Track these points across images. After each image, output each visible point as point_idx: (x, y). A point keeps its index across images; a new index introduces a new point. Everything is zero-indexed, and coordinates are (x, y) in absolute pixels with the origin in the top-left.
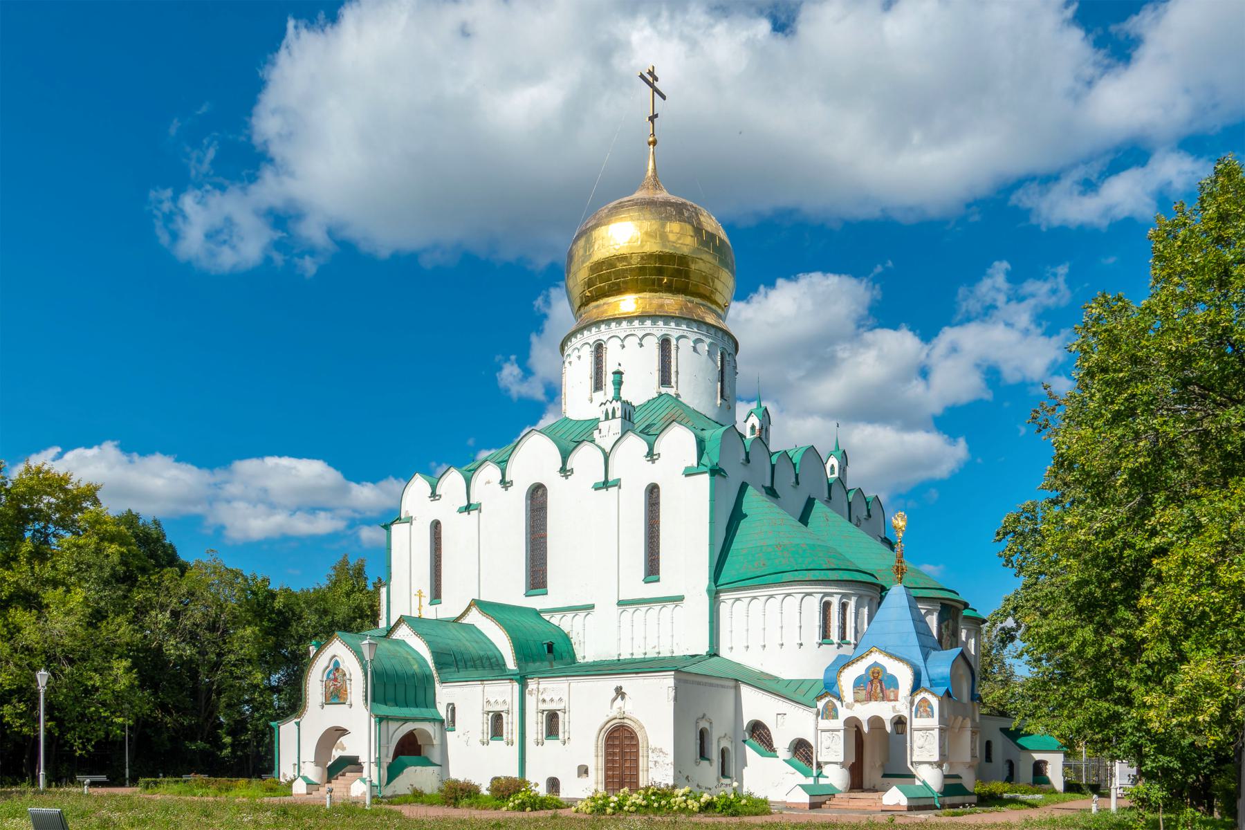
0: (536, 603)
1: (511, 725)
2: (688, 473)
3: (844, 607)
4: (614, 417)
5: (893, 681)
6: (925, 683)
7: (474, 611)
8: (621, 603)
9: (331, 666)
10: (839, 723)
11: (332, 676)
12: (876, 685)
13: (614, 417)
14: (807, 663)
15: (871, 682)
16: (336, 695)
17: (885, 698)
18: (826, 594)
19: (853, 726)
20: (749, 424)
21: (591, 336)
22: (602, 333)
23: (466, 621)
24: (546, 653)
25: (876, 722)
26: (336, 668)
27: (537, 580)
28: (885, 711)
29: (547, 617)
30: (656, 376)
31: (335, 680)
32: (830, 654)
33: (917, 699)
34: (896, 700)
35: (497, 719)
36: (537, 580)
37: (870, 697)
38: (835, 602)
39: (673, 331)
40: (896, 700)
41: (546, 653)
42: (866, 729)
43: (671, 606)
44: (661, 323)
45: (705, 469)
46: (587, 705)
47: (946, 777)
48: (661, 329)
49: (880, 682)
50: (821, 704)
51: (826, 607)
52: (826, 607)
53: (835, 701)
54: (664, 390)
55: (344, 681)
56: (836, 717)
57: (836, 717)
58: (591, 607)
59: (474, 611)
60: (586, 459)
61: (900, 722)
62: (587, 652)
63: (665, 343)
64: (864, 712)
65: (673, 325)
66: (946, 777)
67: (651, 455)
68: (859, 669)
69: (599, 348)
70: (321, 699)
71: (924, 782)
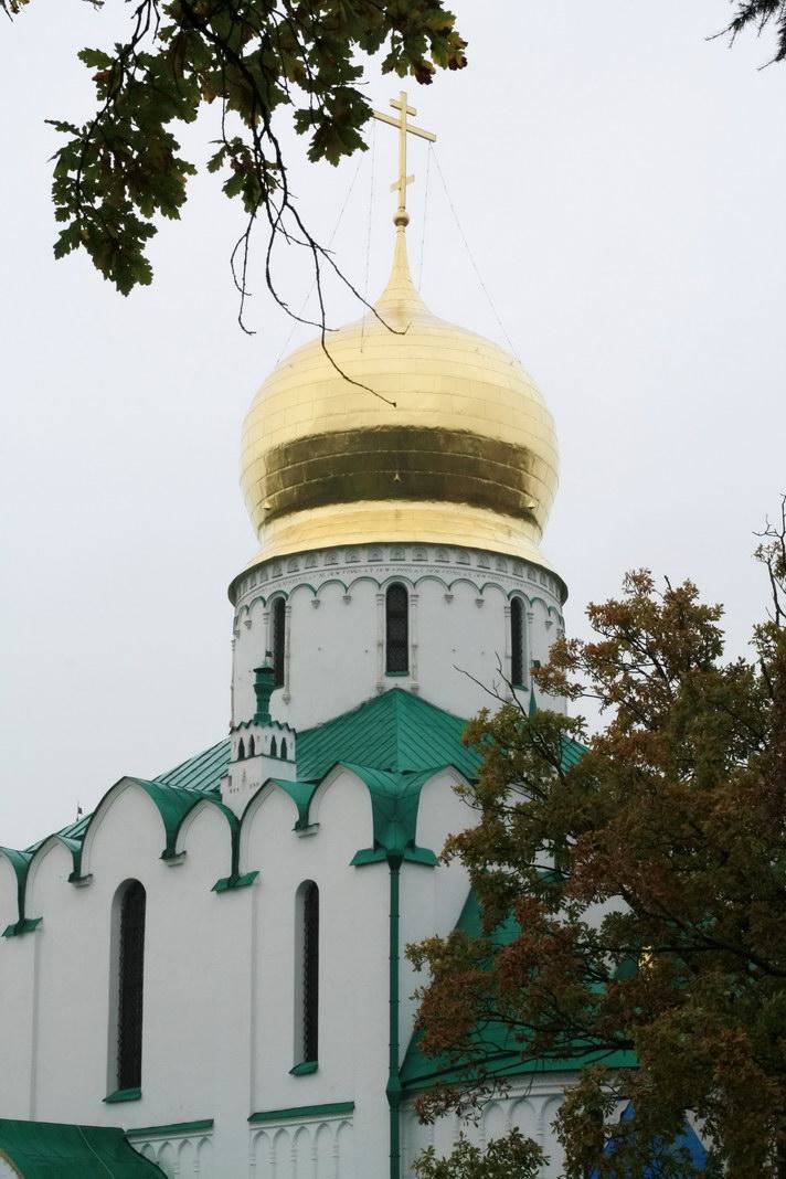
0: (126, 1117)
8: (255, 1118)
13: (252, 755)
21: (267, 587)
30: (378, 659)
43: (334, 1123)
54: (392, 682)
58: (208, 1125)
60: (206, 835)
69: (280, 609)
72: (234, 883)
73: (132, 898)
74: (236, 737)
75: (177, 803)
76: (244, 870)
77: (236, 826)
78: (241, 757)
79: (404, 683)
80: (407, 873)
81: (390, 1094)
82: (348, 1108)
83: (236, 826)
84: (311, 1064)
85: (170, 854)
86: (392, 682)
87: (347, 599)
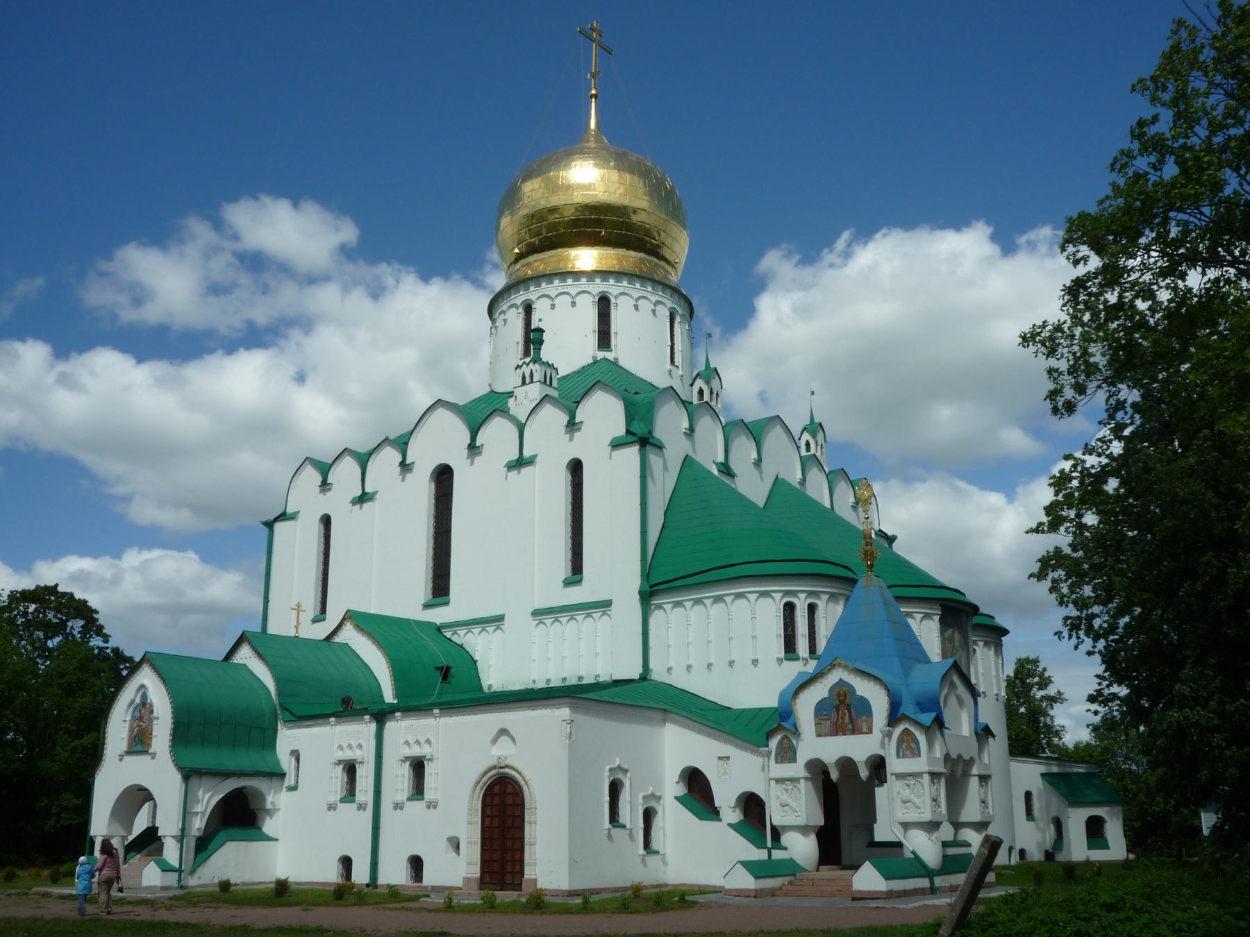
0: (438, 616)
1: (365, 776)
2: (616, 445)
3: (812, 609)
4: (532, 381)
5: (865, 707)
6: (908, 708)
7: (349, 629)
9: (138, 700)
10: (797, 769)
11: (137, 714)
12: (843, 713)
13: (532, 381)
14: (757, 681)
15: (837, 708)
16: (140, 742)
17: (856, 730)
18: (787, 593)
19: (817, 770)
20: (696, 388)
21: (519, 298)
22: (532, 294)
23: (338, 639)
24: (440, 679)
25: (847, 764)
26: (143, 709)
27: (440, 586)
28: (859, 748)
29: (448, 635)
30: (593, 339)
31: (141, 719)
32: (793, 670)
33: (898, 731)
34: (870, 731)
35: (350, 769)
36: (440, 586)
37: (837, 730)
38: (801, 605)
39: (612, 287)
40: (870, 731)
41: (440, 679)
42: (834, 775)
44: (598, 281)
45: (634, 439)
46: (461, 749)
47: (945, 845)
48: (598, 287)
49: (848, 708)
50: (774, 743)
51: (789, 609)
52: (789, 609)
53: (790, 736)
54: (601, 355)
55: (151, 720)
56: (793, 759)
57: (793, 759)
59: (349, 629)
60: (497, 434)
61: (878, 766)
62: (494, 677)
63: (604, 304)
64: (832, 749)
65: (612, 281)
66: (945, 845)
67: (572, 426)
68: (819, 691)
69: (528, 309)
70: (124, 746)
71: (913, 852)
72: (520, 463)
73: (443, 476)
74: (520, 372)
75: (480, 413)
76: (527, 453)
77: (521, 428)
78: (524, 383)
79: (610, 356)
80: (648, 448)
81: (640, 593)
82: (607, 604)
83: (521, 428)
84: (577, 578)
85: (473, 449)
86: (601, 355)
87: (573, 304)
